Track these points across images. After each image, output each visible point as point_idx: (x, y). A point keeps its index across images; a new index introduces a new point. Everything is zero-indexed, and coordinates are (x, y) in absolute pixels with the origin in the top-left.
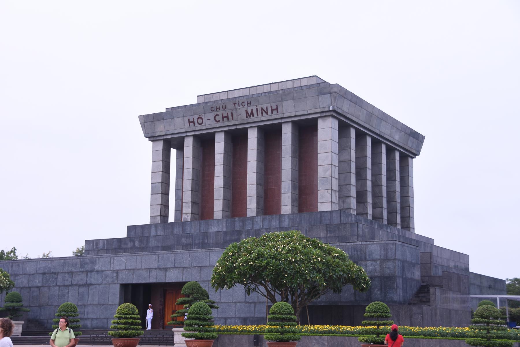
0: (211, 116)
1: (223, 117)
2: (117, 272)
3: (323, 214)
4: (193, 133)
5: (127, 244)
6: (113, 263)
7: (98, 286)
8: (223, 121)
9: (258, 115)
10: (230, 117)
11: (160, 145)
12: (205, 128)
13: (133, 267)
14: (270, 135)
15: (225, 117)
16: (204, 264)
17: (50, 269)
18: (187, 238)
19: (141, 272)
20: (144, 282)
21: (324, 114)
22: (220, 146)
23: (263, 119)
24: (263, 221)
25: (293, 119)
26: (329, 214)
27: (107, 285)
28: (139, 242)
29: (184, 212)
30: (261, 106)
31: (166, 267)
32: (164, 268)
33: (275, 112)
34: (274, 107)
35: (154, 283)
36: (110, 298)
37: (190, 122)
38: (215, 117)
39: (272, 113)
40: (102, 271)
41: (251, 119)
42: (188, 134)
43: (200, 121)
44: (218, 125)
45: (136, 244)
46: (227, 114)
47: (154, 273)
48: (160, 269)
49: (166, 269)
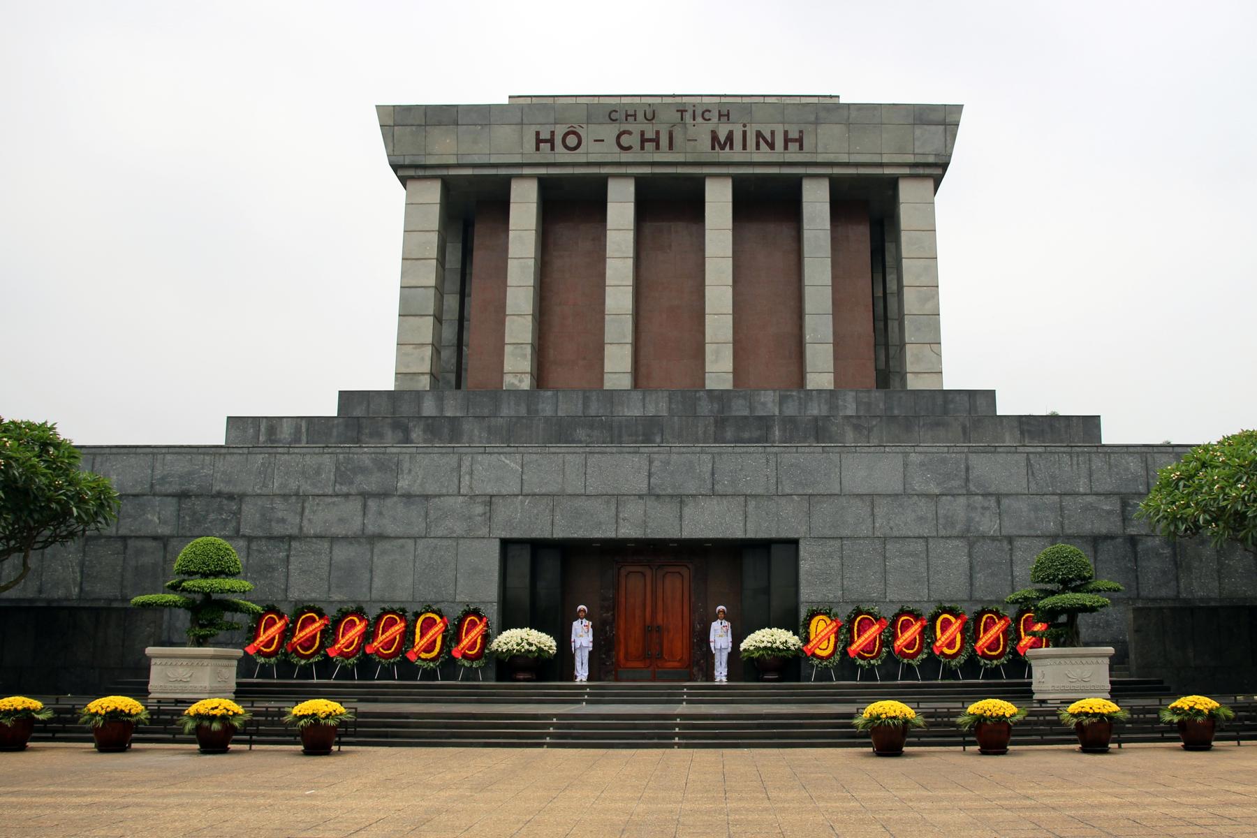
0: (609, 132)
2: (490, 500)
3: (950, 396)
4: (543, 171)
6: (471, 473)
7: (410, 543)
8: (642, 148)
9: (744, 147)
10: (664, 141)
12: (584, 160)
13: (553, 488)
15: (650, 140)
16: (821, 489)
17: (183, 482)
18: (592, 427)
19: (579, 503)
20: (597, 534)
21: (921, 171)
23: (757, 158)
24: (781, 404)
25: (837, 171)
26: (966, 398)
27: (445, 543)
28: (425, 432)
30: (757, 127)
31: (681, 491)
32: (672, 496)
33: (793, 147)
34: (794, 134)
35: (636, 540)
36: (461, 581)
37: (539, 141)
38: (619, 137)
39: (786, 148)
40: (427, 497)
41: (726, 155)
42: (526, 171)
43: (572, 141)
45: (414, 436)
46: (658, 133)
47: (633, 510)
48: (658, 496)
49: (681, 499)
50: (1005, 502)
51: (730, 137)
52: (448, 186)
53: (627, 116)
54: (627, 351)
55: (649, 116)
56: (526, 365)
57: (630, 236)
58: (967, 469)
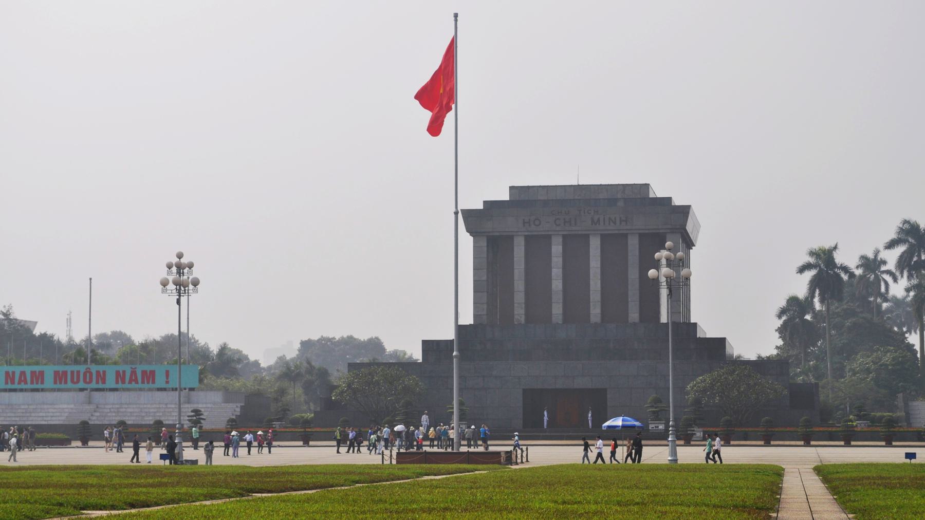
1: (565, 222)
11: (484, 243)
14: (613, 243)
22: (557, 249)
29: (516, 312)
37: (524, 223)
43: (537, 222)
44: (558, 228)
51: (599, 220)
52: (488, 237)
54: (561, 305)
56: (522, 312)
57: (561, 259)
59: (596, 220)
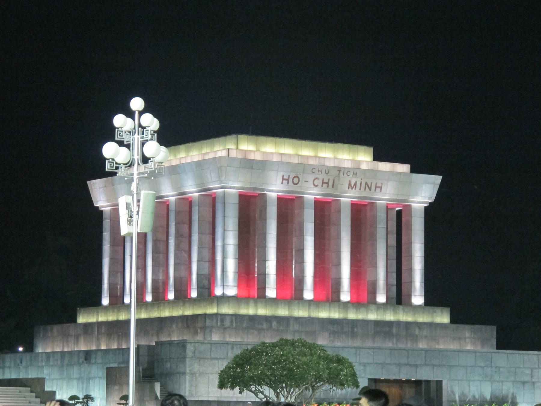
1: (323, 183)
5: (262, 324)
6: (359, 355)
8: (322, 186)
9: (360, 189)
15: (326, 183)
37: (283, 179)
38: (314, 180)
39: (375, 190)
43: (296, 180)
46: (329, 180)
48: (410, 365)
49: (416, 366)
50: (501, 369)
51: (355, 185)
53: (319, 171)
55: (327, 172)
58: (492, 358)
59: (352, 185)
